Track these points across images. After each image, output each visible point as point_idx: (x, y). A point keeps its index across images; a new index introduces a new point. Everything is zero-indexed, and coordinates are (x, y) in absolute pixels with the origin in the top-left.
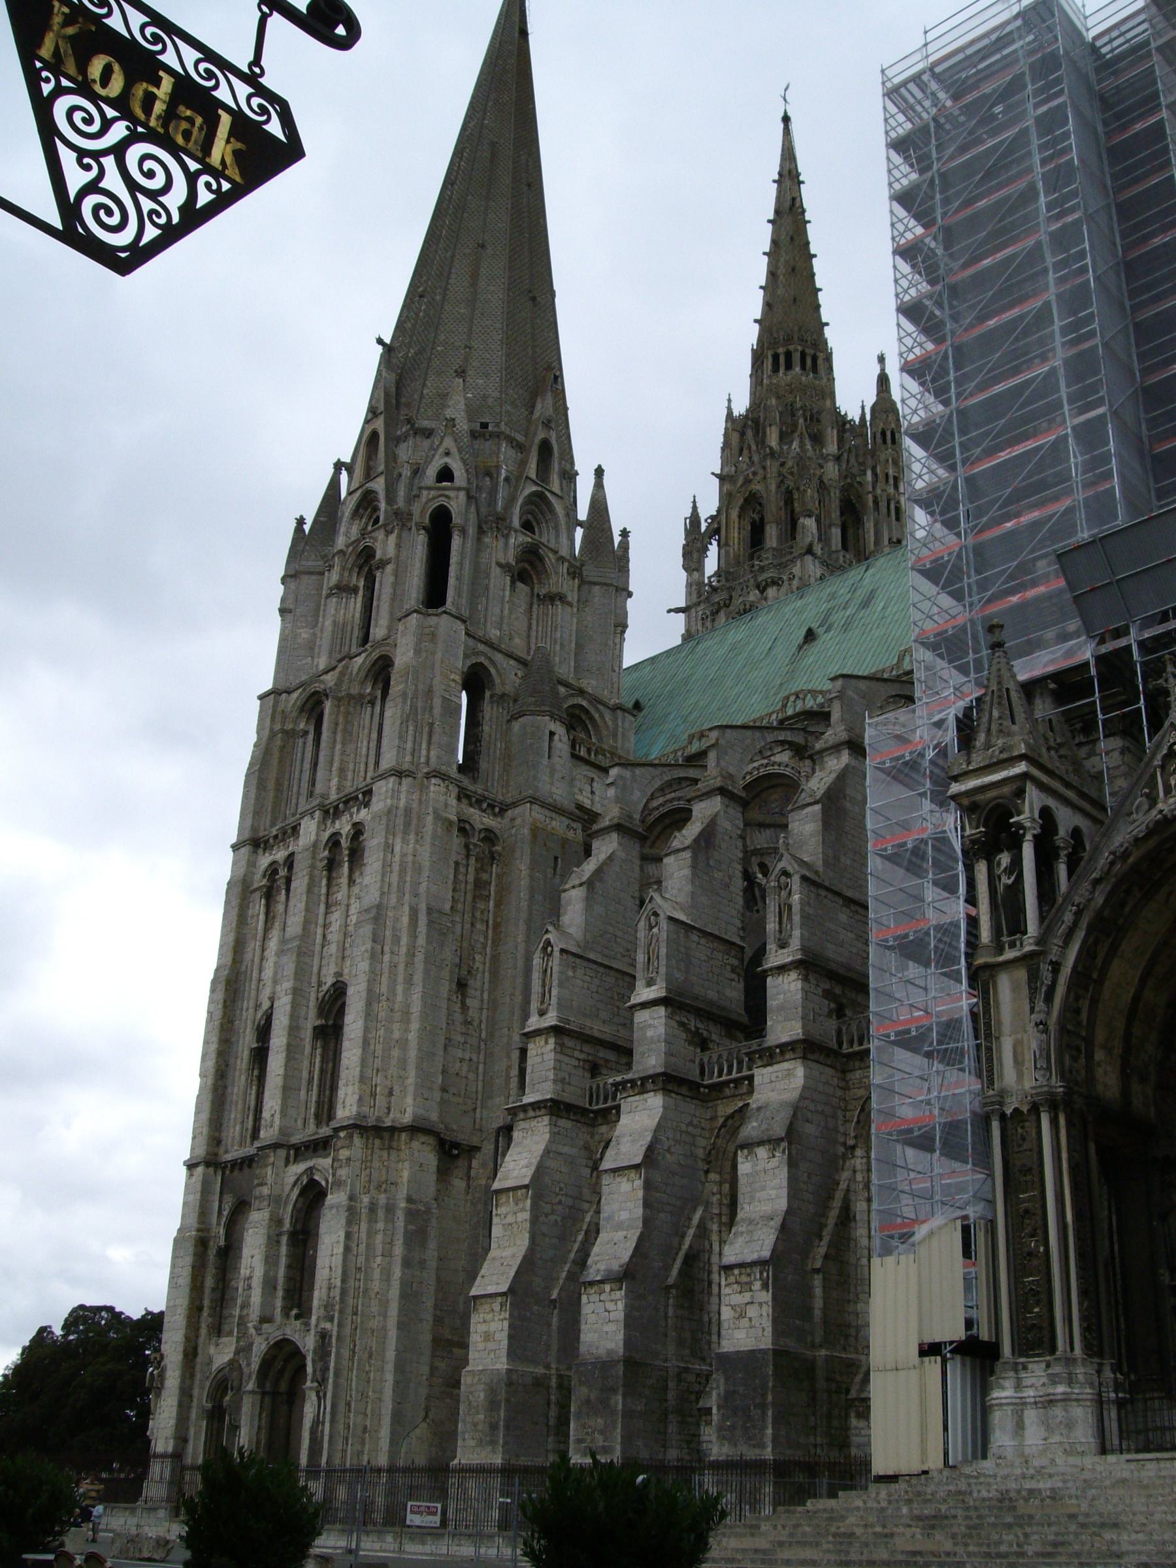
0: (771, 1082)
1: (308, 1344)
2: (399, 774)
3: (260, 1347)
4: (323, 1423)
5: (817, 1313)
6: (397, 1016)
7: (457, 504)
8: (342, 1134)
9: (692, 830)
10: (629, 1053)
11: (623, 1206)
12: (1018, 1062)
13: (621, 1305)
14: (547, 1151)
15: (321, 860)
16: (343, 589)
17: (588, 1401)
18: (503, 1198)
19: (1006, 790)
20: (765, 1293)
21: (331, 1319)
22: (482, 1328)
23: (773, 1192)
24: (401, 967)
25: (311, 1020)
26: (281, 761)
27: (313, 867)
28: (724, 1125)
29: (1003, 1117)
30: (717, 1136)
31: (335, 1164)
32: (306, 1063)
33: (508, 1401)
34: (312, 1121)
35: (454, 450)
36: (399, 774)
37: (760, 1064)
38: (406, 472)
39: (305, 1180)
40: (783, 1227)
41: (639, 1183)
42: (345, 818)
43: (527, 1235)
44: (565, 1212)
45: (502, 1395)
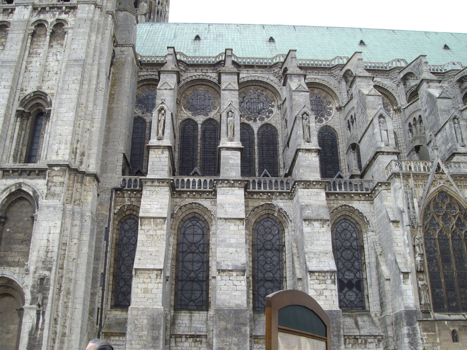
0: (308, 196)
4: (42, 329)
8: (56, 169)
13: (244, 283)
15: (29, 30)
17: (226, 329)
18: (146, 222)
20: (333, 285)
21: (50, 270)
23: (324, 243)
24: (92, 94)
28: (253, 210)
30: (249, 215)
31: (50, 184)
32: (11, 127)
34: (11, 158)
37: (302, 187)
39: (13, 189)
43: (165, 242)
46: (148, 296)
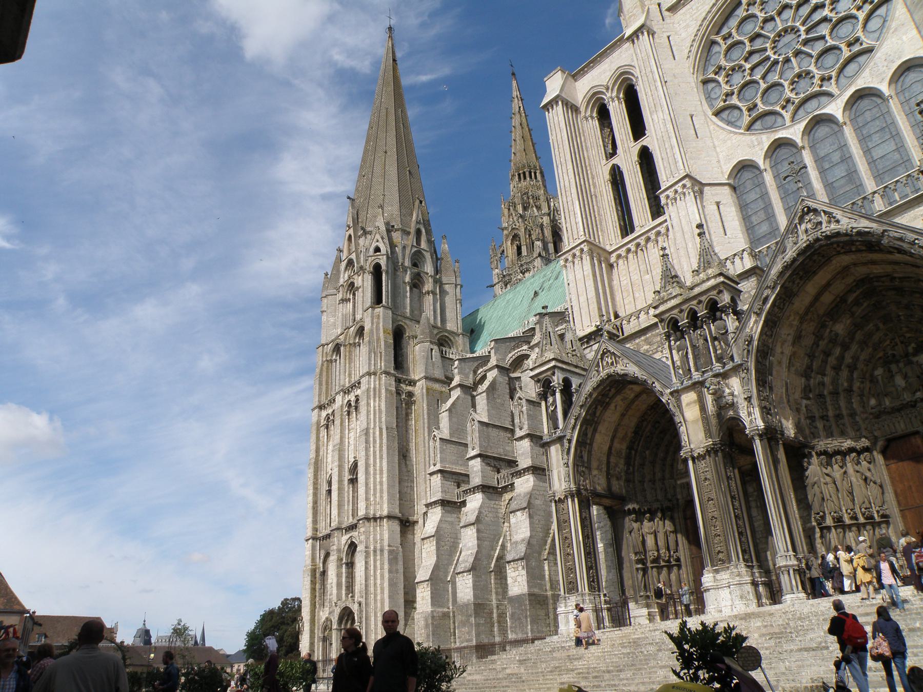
1: (355, 608)
2: (369, 374)
3: (337, 611)
5: (547, 577)
6: (378, 472)
7: (383, 262)
9: (486, 384)
10: (468, 476)
11: (469, 540)
12: (560, 480)
13: (471, 581)
14: (441, 521)
16: (344, 301)
19: (549, 373)
22: (421, 595)
25: (347, 476)
26: (327, 372)
27: (342, 415)
29: (556, 502)
33: (432, 624)
35: (380, 240)
36: (369, 374)
38: (364, 250)
40: (529, 543)
41: (475, 530)
42: (352, 394)
44: (446, 543)
45: (430, 621)
46: (424, 602)
